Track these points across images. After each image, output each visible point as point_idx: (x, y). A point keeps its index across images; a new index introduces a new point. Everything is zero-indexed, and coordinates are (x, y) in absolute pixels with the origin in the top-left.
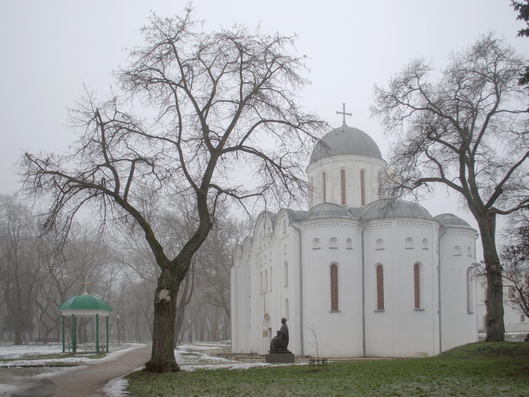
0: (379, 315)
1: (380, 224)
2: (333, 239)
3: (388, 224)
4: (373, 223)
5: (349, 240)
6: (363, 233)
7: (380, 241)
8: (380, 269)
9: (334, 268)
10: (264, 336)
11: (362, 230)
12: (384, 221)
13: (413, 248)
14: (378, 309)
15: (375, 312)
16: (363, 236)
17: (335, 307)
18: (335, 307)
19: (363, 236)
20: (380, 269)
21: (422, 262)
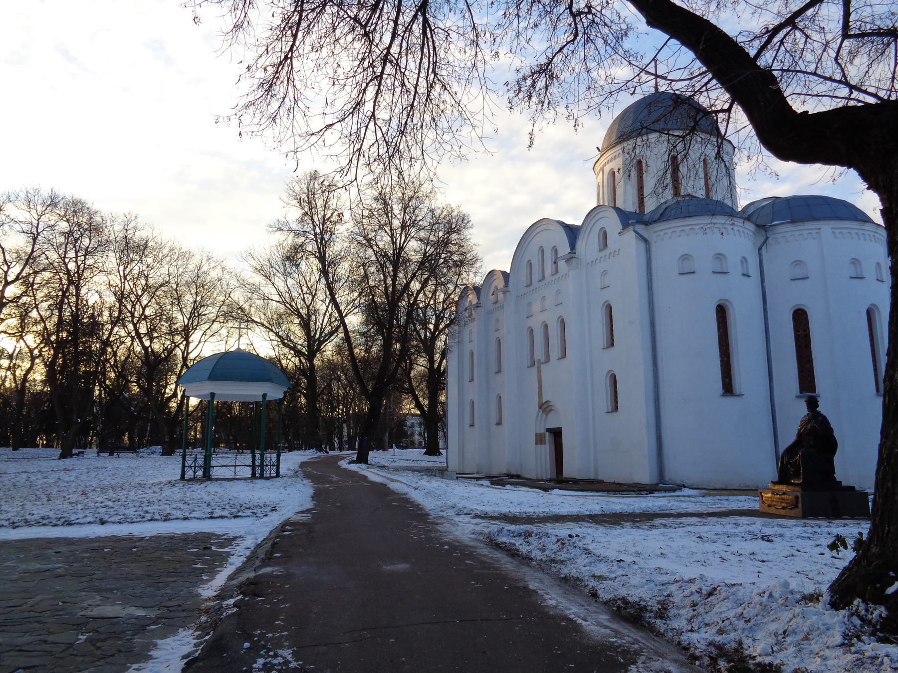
0: (615, 415)
1: (797, 233)
2: (719, 256)
3: (814, 232)
4: (786, 230)
5: (744, 260)
6: (760, 249)
7: (798, 263)
8: (800, 318)
9: (722, 312)
10: (536, 443)
11: (759, 245)
12: (806, 227)
13: (863, 278)
14: (801, 392)
15: (797, 397)
16: (760, 256)
17: (728, 388)
18: (728, 388)
19: (760, 256)
20: (800, 318)
21: (877, 305)
